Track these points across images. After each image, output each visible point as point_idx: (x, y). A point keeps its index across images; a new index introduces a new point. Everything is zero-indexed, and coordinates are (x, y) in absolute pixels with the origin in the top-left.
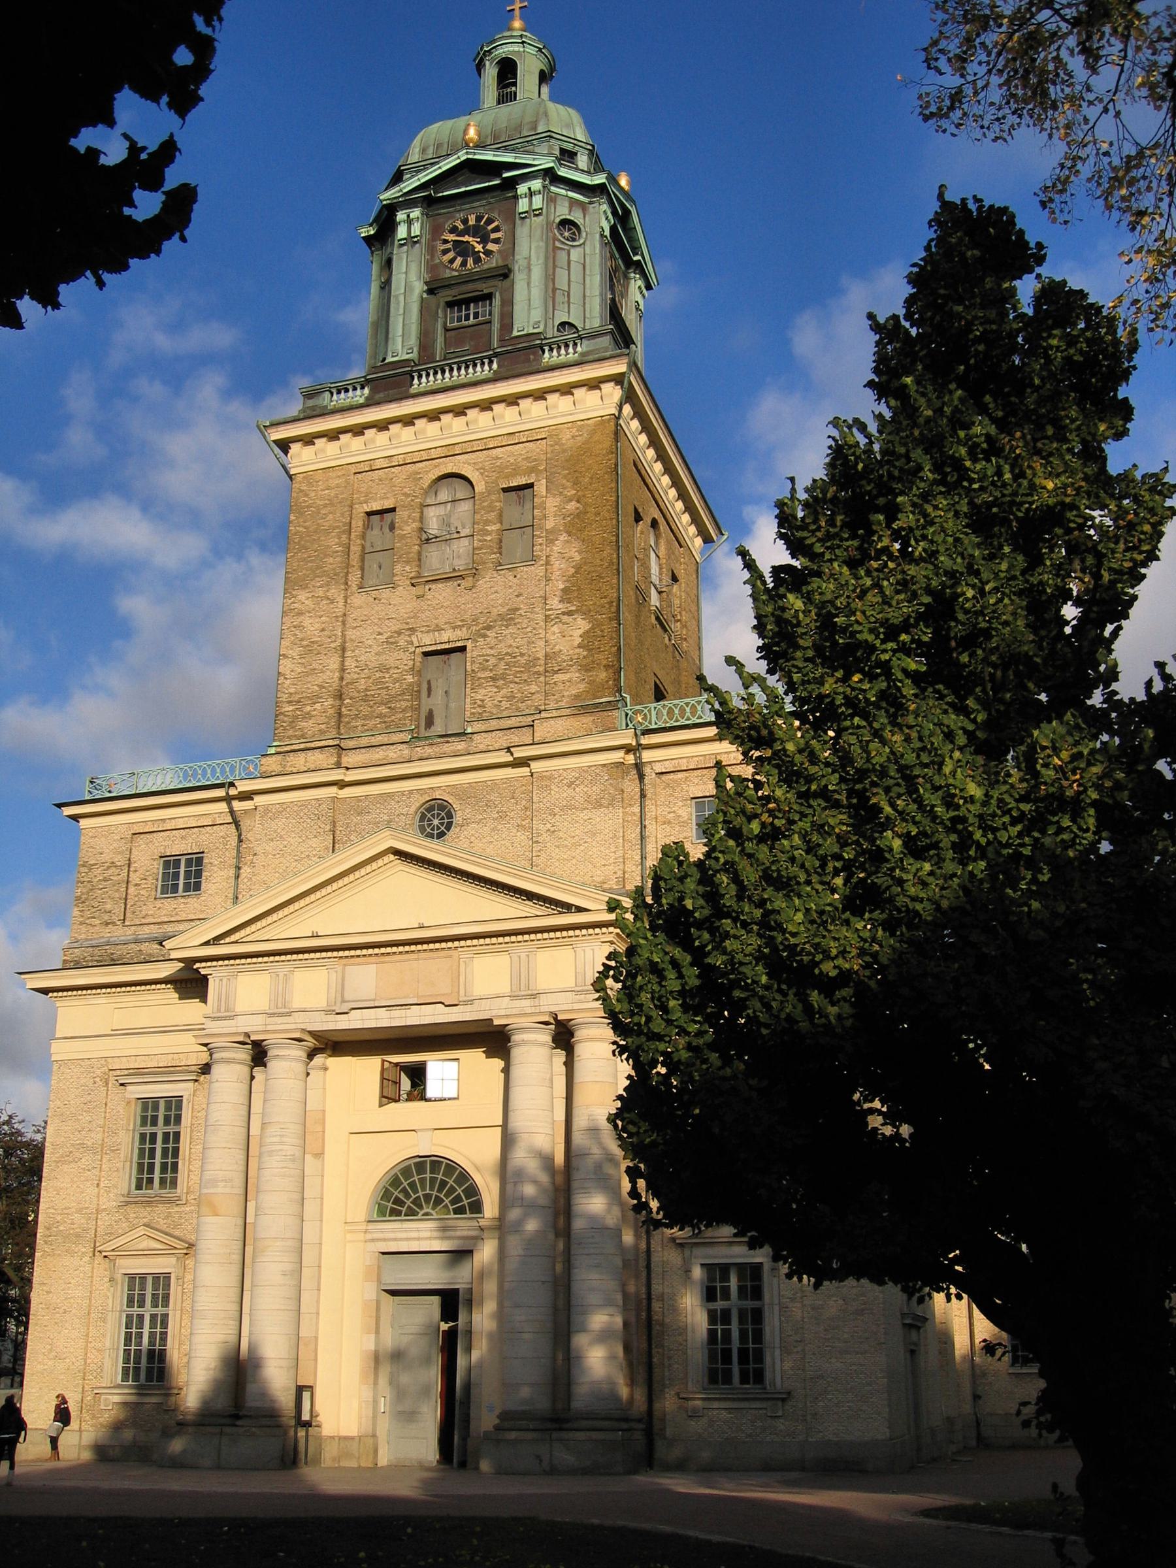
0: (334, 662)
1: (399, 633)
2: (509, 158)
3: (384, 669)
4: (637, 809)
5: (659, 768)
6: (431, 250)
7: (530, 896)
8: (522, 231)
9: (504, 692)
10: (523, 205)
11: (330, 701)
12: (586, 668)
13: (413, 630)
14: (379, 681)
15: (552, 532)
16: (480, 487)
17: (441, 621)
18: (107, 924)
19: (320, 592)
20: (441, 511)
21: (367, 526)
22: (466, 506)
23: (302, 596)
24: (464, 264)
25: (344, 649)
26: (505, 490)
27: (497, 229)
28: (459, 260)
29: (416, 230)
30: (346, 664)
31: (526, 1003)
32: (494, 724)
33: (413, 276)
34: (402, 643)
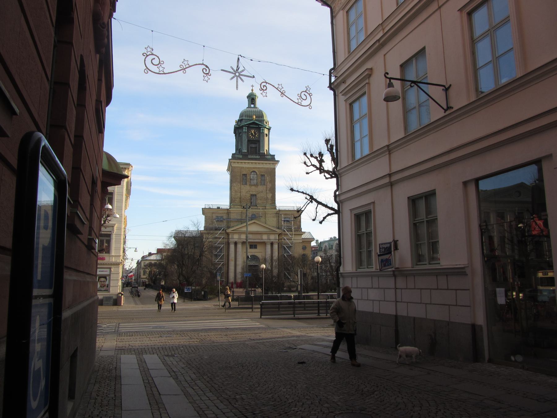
0: (239, 194)
1: (248, 191)
2: (260, 124)
3: (246, 196)
4: (278, 218)
5: (280, 214)
6: (248, 134)
7: (270, 229)
8: (261, 135)
9: (261, 201)
10: (261, 131)
11: (239, 199)
12: (272, 200)
13: (249, 191)
14: (245, 197)
15: (267, 182)
16: (258, 174)
17: (253, 191)
18: (210, 224)
19: (237, 184)
20: (252, 175)
21: (243, 175)
22: (255, 176)
23: (234, 184)
24: (253, 137)
25: (240, 192)
26: (261, 175)
27: (257, 133)
28: (252, 137)
29: (246, 130)
30: (241, 194)
31: (269, 240)
32: (261, 205)
33: (246, 138)
34: (248, 193)
